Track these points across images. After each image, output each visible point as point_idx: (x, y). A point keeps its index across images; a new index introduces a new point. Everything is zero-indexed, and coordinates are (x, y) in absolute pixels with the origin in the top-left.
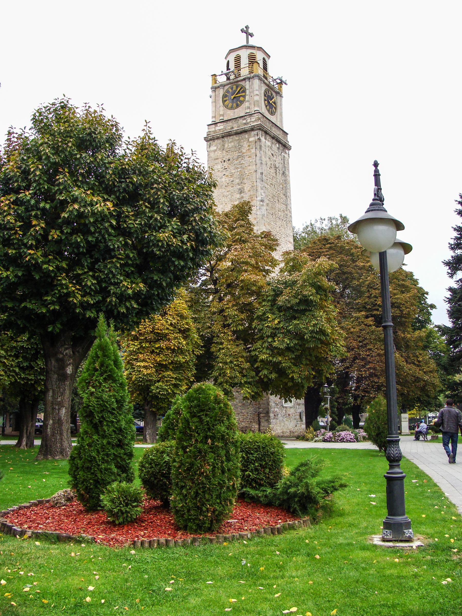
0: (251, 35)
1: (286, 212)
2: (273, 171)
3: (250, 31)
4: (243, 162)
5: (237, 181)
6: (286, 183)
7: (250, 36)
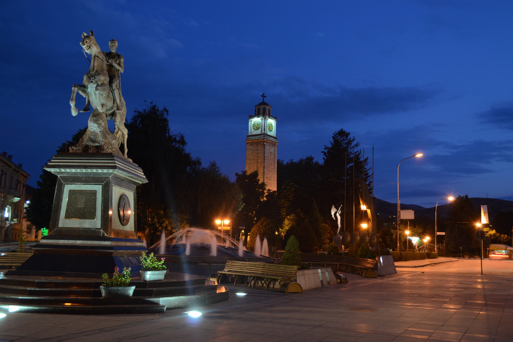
0: (265, 97)
1: (274, 169)
2: (270, 154)
3: (265, 95)
4: (258, 152)
5: (256, 158)
6: (275, 158)
7: (264, 98)
